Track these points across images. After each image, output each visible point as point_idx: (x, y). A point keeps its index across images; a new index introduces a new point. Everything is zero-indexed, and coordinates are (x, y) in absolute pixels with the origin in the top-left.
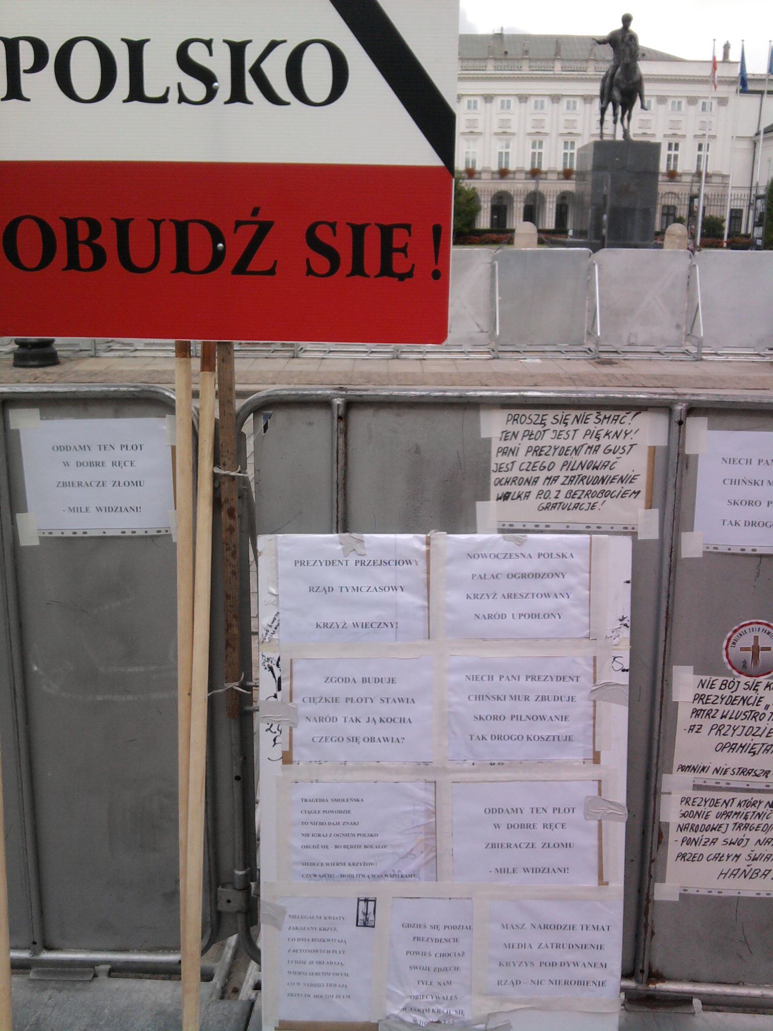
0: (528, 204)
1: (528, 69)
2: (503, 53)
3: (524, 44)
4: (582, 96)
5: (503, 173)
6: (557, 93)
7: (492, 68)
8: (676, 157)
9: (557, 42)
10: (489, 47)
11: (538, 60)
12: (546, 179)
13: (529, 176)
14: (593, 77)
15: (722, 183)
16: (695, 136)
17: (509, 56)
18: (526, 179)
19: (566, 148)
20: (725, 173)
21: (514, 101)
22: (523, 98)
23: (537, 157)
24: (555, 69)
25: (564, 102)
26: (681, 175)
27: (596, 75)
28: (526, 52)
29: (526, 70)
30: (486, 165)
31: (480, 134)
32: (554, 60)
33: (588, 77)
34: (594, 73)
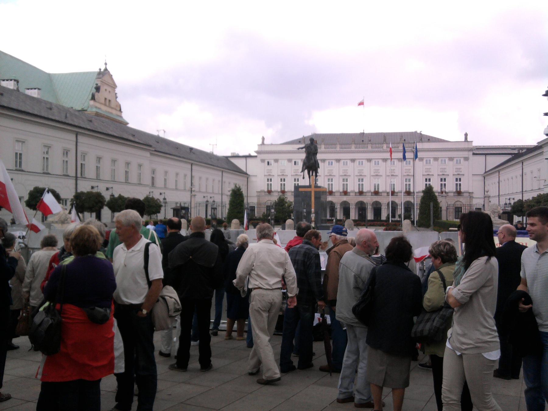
2: (362, 141)
4: (397, 159)
5: (361, 193)
6: (421, 157)
7: (339, 148)
8: (271, 184)
9: (384, 136)
12: (381, 195)
13: (373, 194)
15: (469, 196)
16: (453, 175)
17: (364, 142)
18: (372, 195)
20: (470, 191)
23: (361, 186)
26: (463, 193)
28: (370, 141)
29: (370, 148)
32: (383, 144)
33: (399, 150)
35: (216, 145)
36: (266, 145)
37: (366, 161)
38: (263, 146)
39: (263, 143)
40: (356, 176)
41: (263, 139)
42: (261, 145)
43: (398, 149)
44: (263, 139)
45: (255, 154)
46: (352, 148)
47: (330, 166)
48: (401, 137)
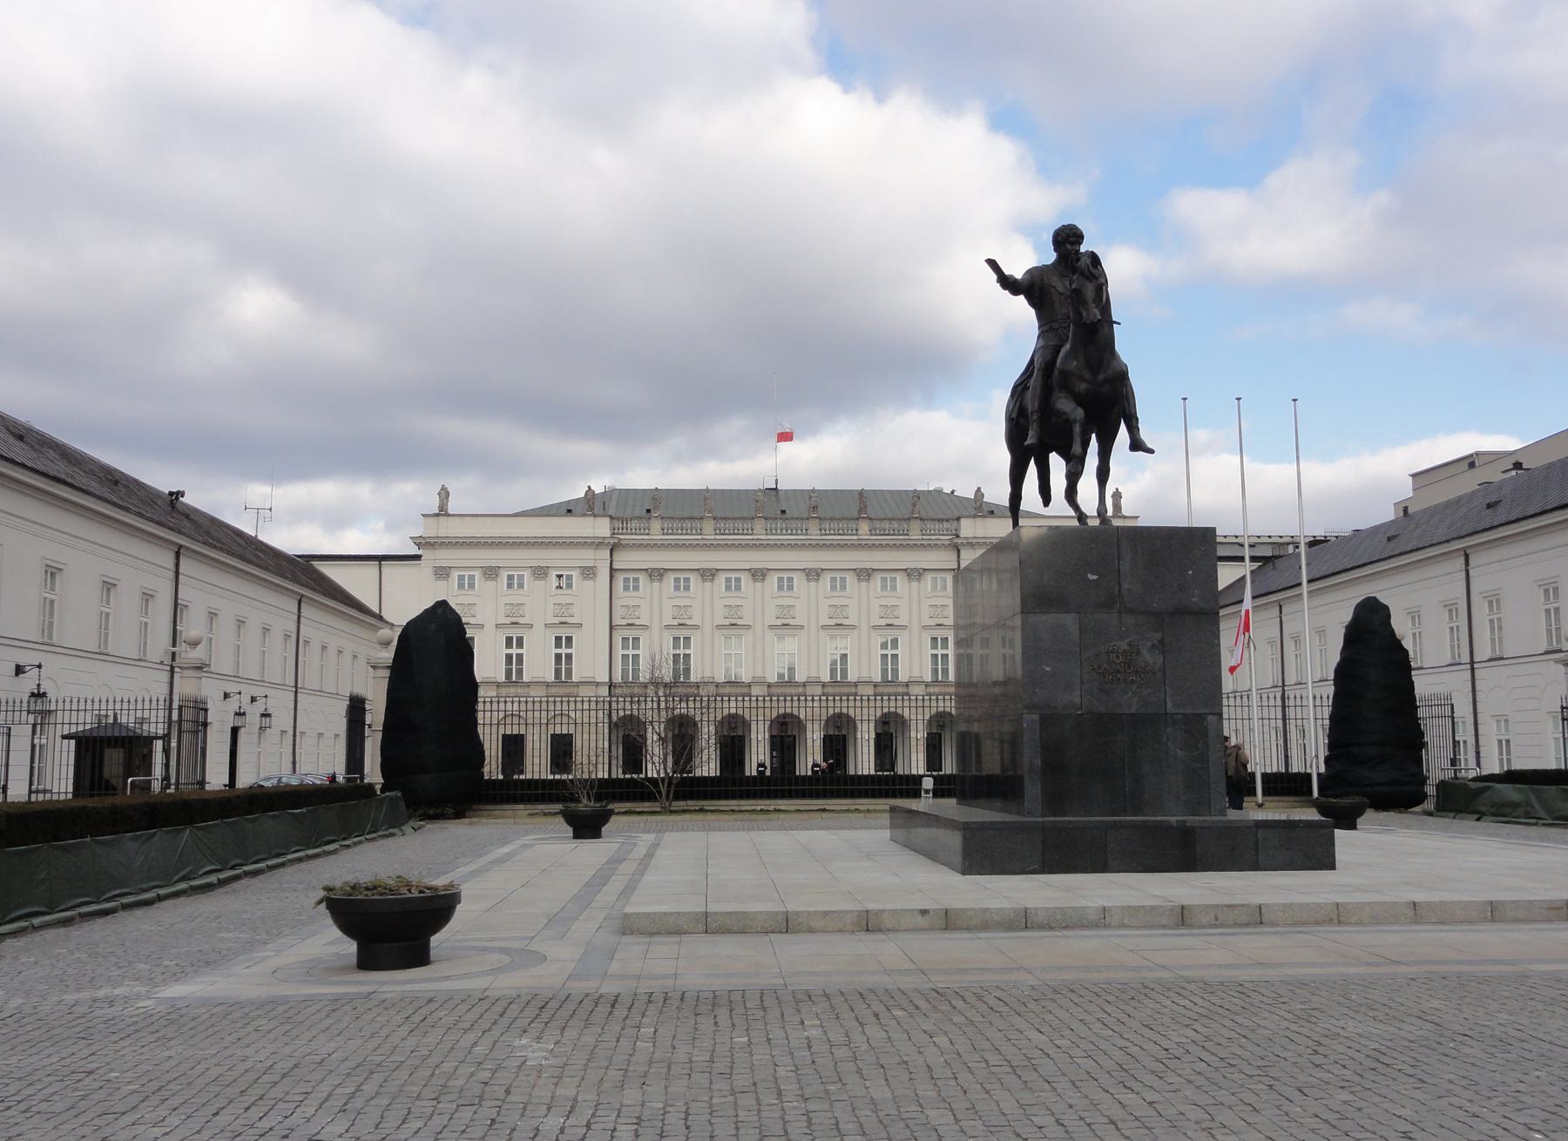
0: (831, 732)
1: (819, 532)
3: (810, 498)
10: (757, 501)
11: (832, 519)
14: (919, 543)
19: (934, 646)
21: (798, 579)
22: (813, 574)
24: (859, 532)
25: (877, 579)
27: (922, 539)
28: (815, 508)
30: (759, 674)
31: (748, 627)
32: (858, 519)
34: (920, 537)
35: (271, 509)
36: (453, 515)
37: (803, 575)
38: (442, 519)
39: (443, 512)
40: (772, 627)
41: (444, 494)
42: (437, 515)
43: (907, 537)
44: (444, 494)
45: (414, 551)
46: (754, 531)
47: (682, 593)
48: (916, 499)
